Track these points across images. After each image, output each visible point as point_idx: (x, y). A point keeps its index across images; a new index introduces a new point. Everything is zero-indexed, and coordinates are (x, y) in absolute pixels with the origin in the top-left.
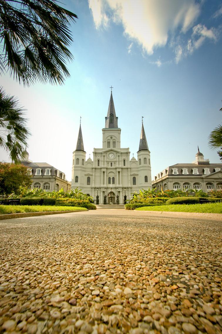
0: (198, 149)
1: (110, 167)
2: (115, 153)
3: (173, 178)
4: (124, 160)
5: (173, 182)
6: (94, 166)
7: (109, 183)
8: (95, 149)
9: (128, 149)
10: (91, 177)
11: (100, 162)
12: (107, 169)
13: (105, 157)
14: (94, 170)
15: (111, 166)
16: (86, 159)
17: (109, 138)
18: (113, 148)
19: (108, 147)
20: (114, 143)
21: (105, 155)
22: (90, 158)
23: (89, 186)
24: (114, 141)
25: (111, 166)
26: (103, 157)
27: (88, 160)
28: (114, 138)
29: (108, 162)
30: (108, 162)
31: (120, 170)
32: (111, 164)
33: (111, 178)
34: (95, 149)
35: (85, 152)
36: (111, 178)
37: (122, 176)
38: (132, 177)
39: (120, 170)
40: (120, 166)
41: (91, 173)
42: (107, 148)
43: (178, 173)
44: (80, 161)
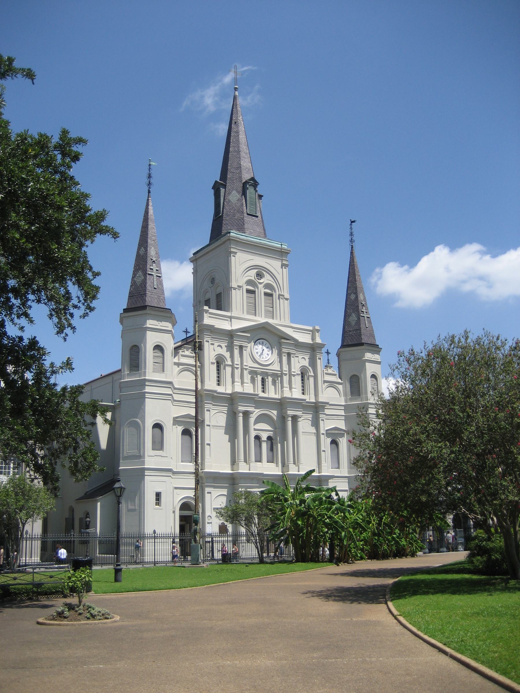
4: (303, 374)
29: (253, 373)
30: (253, 373)
32: (263, 381)
33: (264, 436)
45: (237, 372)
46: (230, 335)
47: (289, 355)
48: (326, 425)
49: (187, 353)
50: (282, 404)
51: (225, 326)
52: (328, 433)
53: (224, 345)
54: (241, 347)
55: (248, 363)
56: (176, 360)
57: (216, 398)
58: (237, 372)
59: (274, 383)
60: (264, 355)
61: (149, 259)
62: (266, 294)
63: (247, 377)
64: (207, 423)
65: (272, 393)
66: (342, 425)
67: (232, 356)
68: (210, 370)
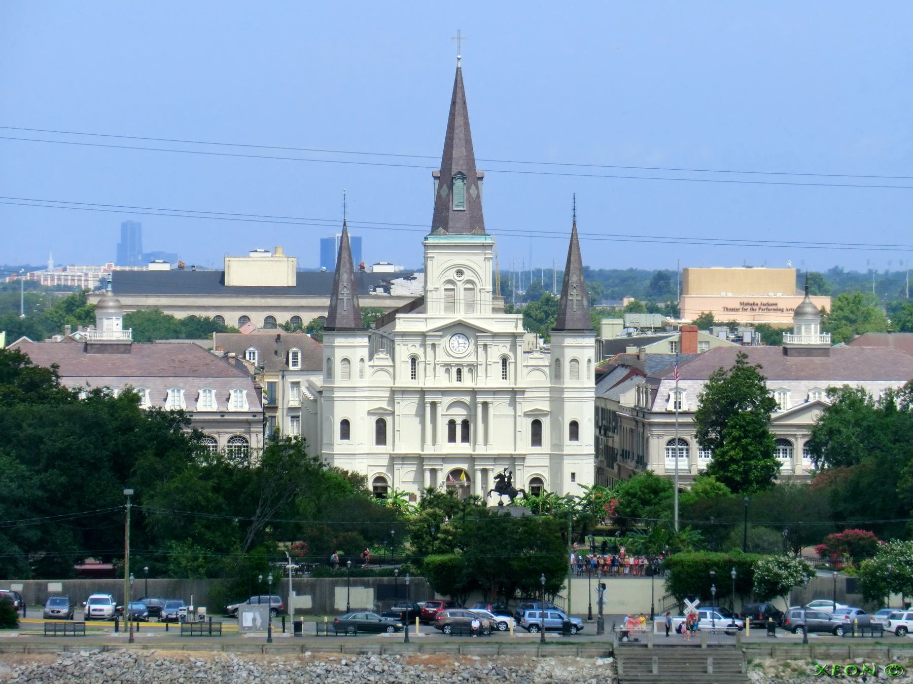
4: (505, 361)
5: (668, 438)
7: (452, 438)
11: (420, 368)
15: (459, 379)
17: (452, 275)
19: (447, 310)
23: (381, 449)
25: (459, 379)
26: (429, 349)
29: (447, 367)
30: (447, 367)
32: (459, 372)
33: (459, 421)
36: (459, 421)
42: (443, 314)
45: (430, 368)
46: (424, 335)
47: (485, 346)
48: (525, 406)
49: (382, 355)
50: (474, 393)
51: (421, 327)
52: (526, 415)
53: (417, 345)
54: (434, 345)
55: (442, 358)
56: (371, 363)
57: (404, 392)
58: (430, 368)
59: (470, 371)
60: (459, 348)
61: (340, 286)
62: (466, 289)
63: (441, 371)
64: (396, 413)
65: (467, 382)
66: (545, 406)
67: (425, 353)
68: (404, 369)
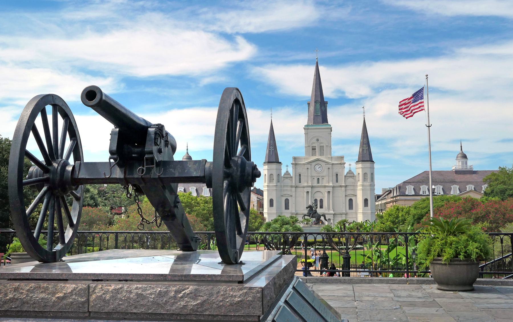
0: (461, 147)
1: (315, 184)
2: (323, 164)
3: (405, 200)
6: (294, 185)
8: (295, 159)
9: (342, 158)
10: (289, 198)
12: (312, 187)
13: (310, 170)
14: (294, 189)
15: (318, 182)
16: (283, 172)
17: (314, 140)
18: (320, 157)
20: (322, 148)
21: (309, 166)
22: (287, 172)
24: (322, 145)
25: (318, 182)
27: (285, 174)
28: (321, 140)
31: (330, 189)
32: (318, 179)
34: (295, 159)
35: (280, 163)
37: (333, 197)
38: (348, 198)
39: (330, 189)
40: (331, 184)
41: (289, 193)
43: (413, 193)
44: (275, 177)
46: (304, 164)
